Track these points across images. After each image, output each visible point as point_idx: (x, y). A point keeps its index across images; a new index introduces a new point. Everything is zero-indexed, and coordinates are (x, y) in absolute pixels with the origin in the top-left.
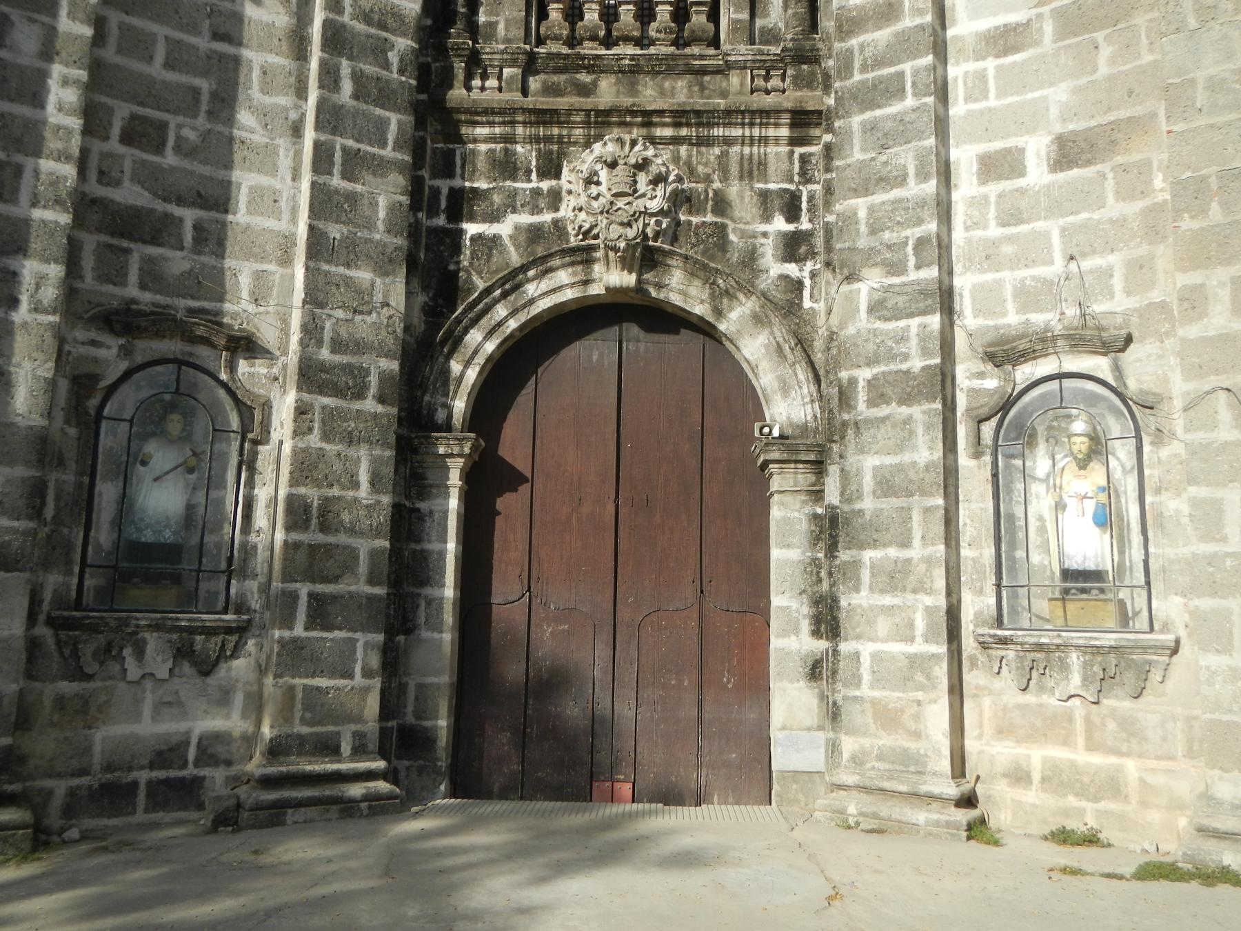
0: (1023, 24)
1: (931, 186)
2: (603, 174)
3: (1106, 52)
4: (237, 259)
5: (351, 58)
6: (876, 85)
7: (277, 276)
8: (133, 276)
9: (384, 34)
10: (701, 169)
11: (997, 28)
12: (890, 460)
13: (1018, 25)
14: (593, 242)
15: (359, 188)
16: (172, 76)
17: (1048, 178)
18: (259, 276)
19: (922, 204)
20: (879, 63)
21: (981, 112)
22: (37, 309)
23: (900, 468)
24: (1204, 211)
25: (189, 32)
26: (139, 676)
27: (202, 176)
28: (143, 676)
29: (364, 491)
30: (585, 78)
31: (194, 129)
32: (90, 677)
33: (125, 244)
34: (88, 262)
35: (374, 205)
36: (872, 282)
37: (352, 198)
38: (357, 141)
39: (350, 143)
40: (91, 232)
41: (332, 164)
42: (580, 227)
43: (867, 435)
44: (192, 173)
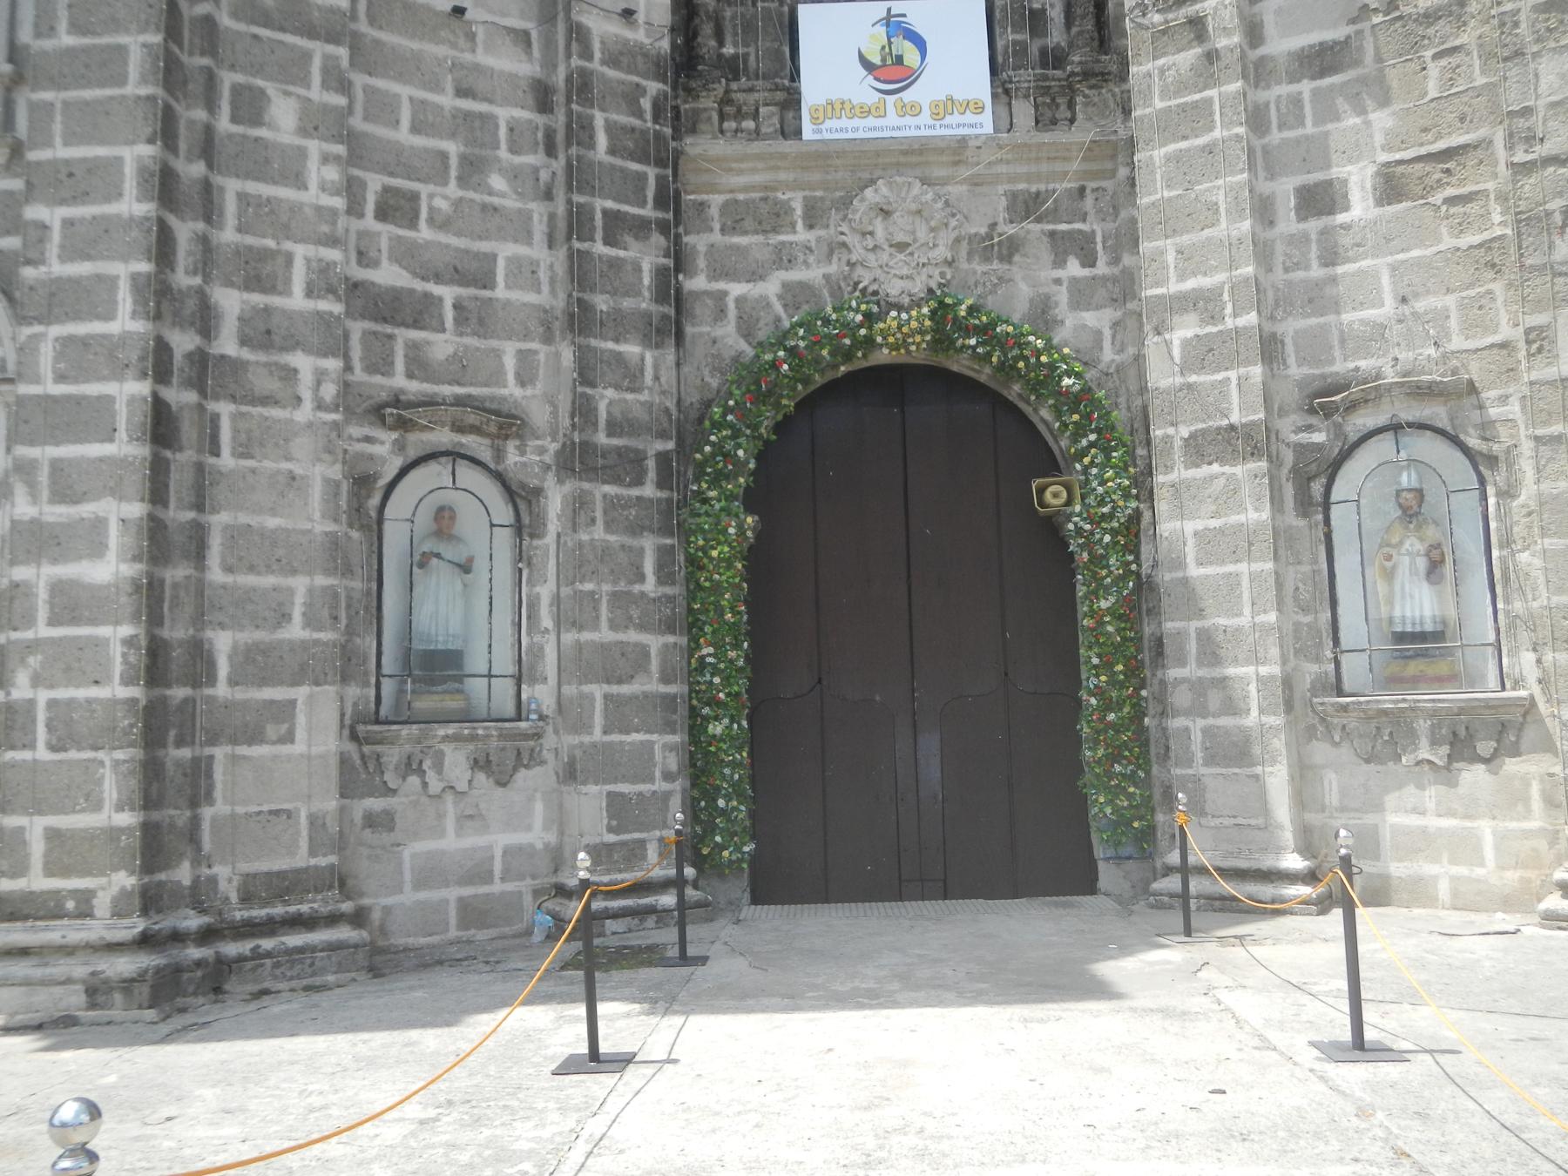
0: (1341, 42)
4: (499, 338)
5: (603, 110)
7: (542, 357)
8: (400, 365)
11: (1311, 46)
13: (1335, 43)
15: (622, 253)
16: (420, 141)
18: (522, 356)
21: (1298, 141)
22: (320, 406)
25: (432, 90)
26: (439, 790)
27: (457, 250)
28: (444, 790)
29: (650, 586)
31: (445, 197)
32: (394, 792)
33: (389, 329)
34: (356, 353)
35: (638, 269)
37: (615, 264)
38: (616, 199)
40: (355, 319)
41: (593, 228)
42: (856, 284)
44: (447, 246)
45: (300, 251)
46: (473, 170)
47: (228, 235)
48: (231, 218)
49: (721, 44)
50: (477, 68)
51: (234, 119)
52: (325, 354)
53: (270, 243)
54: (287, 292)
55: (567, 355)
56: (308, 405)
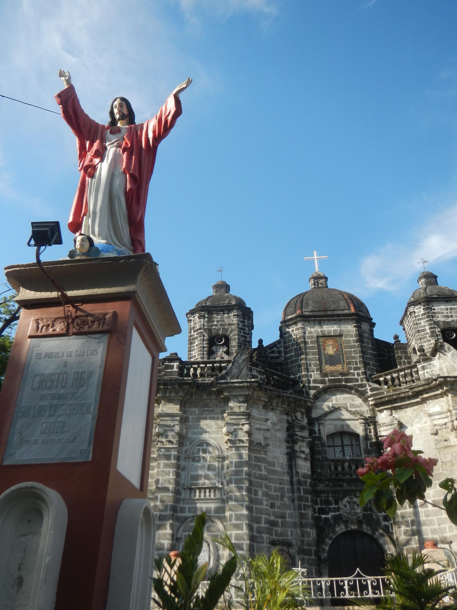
9: (306, 480)
14: (348, 519)
15: (306, 512)
18: (292, 532)
19: (410, 513)
30: (341, 483)
33: (272, 528)
35: (309, 515)
36: (403, 528)
37: (305, 514)
39: (304, 503)
45: (263, 516)
46: (282, 497)
48: (254, 512)
49: (318, 470)
50: (282, 479)
51: (254, 495)
53: (259, 515)
54: (261, 524)
55: (299, 531)
56: (265, 543)
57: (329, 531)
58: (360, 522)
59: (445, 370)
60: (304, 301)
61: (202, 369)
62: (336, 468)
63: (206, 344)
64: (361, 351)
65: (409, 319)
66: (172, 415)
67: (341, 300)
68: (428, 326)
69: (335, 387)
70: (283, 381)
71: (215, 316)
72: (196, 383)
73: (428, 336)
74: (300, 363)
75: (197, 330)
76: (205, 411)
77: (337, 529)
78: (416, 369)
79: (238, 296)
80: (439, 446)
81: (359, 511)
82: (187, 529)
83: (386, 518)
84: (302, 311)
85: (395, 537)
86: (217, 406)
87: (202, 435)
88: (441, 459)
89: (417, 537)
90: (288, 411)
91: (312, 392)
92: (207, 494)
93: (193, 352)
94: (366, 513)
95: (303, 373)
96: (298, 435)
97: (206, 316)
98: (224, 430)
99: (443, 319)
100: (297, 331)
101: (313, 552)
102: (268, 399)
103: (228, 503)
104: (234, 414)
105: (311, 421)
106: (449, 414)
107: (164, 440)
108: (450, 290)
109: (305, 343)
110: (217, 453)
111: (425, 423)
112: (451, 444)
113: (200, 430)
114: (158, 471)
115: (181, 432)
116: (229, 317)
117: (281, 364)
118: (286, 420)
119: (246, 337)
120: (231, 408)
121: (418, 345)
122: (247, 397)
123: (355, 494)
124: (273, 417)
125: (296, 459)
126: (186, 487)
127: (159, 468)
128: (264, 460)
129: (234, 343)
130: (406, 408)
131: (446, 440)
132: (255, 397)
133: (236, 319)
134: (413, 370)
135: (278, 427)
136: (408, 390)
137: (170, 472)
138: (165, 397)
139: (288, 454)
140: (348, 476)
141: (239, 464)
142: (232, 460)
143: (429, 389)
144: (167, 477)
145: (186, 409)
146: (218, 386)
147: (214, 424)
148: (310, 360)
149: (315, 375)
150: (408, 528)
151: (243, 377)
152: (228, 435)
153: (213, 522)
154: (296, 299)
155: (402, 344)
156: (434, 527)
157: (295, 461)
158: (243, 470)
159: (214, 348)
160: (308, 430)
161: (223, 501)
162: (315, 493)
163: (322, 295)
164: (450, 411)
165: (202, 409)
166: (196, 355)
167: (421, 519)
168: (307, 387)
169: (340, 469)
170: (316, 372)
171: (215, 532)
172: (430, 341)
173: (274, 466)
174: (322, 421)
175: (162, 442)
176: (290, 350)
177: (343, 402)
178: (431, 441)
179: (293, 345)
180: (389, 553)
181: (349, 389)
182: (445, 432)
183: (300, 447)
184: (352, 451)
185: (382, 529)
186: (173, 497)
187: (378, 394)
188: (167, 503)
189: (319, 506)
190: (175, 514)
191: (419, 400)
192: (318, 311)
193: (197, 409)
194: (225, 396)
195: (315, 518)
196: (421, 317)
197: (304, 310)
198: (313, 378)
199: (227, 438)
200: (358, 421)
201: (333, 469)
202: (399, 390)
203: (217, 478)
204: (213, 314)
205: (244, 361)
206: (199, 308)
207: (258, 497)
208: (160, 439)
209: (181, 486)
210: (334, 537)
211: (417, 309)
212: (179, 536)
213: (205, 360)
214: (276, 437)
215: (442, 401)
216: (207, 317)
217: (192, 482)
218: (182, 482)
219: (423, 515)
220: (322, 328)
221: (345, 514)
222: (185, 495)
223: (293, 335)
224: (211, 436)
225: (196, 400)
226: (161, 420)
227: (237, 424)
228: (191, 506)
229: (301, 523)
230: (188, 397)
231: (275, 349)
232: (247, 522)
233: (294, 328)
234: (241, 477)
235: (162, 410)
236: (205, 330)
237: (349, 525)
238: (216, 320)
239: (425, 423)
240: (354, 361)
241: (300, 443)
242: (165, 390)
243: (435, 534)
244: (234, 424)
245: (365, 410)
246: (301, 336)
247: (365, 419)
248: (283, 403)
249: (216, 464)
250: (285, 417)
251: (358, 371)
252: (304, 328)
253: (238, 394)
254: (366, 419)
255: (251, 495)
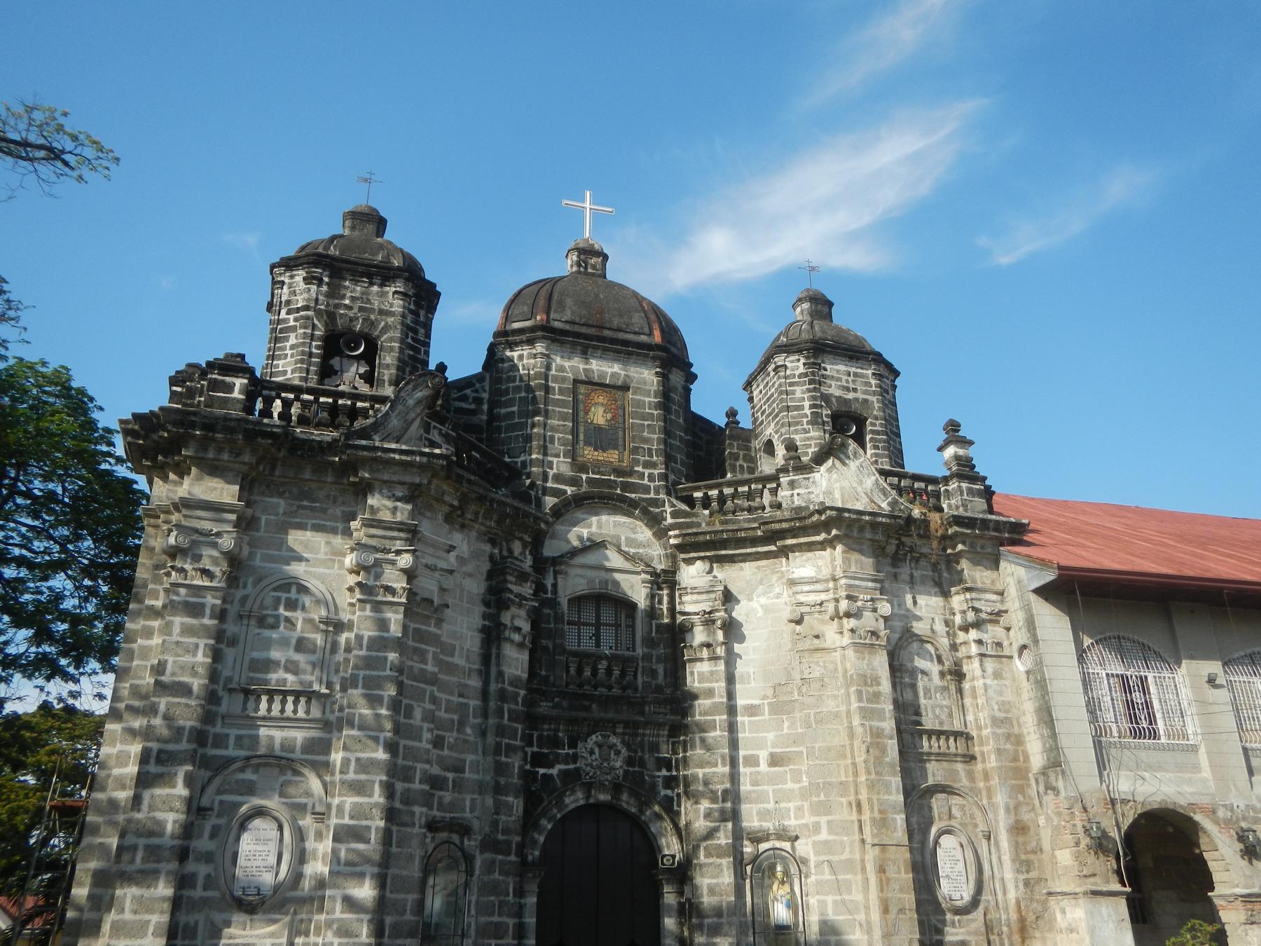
1: (727, 769)
2: (597, 750)
3: (786, 724)
6: (706, 721)
8: (435, 807)
10: (633, 747)
12: (714, 881)
17: (768, 769)
18: (473, 800)
19: (724, 775)
20: (706, 714)
22: (420, 827)
23: (717, 885)
24: (819, 795)
30: (587, 704)
33: (434, 792)
35: (514, 766)
36: (705, 805)
37: (507, 764)
39: (507, 741)
43: (704, 870)
46: (462, 724)
47: (400, 761)
48: (401, 756)
50: (466, 686)
52: (423, 806)
53: (411, 764)
54: (414, 782)
55: (489, 801)
56: (417, 826)
57: (550, 802)
58: (617, 788)
59: (837, 495)
60: (555, 297)
61: (305, 405)
62: (580, 671)
63: (318, 347)
64: (662, 429)
65: (768, 379)
66: (216, 508)
67: (636, 311)
68: (809, 400)
69: (600, 498)
70: (490, 465)
71: (347, 283)
72: (290, 438)
73: (805, 420)
74: (529, 431)
75: (298, 310)
76: (304, 508)
77: (567, 800)
78: (774, 485)
79: (406, 249)
80: (800, 646)
81: (618, 764)
82: (227, 787)
83: (671, 782)
84: (548, 317)
85: (683, 822)
86: (335, 502)
87: (289, 565)
88: (802, 672)
89: (730, 825)
90: (496, 534)
91: (550, 501)
92: (290, 707)
93: (281, 362)
94: (631, 769)
95: (534, 456)
96: (511, 592)
97: (326, 279)
98: (350, 560)
99: (838, 393)
100: (532, 361)
101: (514, 846)
102: (460, 501)
103: (340, 730)
104: (379, 524)
105: (541, 564)
106: (831, 585)
107: (187, 567)
108: (856, 336)
109: (547, 389)
110: (323, 613)
111: (778, 596)
112: (826, 646)
113: (284, 553)
114: (164, 641)
115: (237, 550)
116: (383, 295)
117: (476, 429)
118: (487, 554)
119: (417, 351)
120: (373, 510)
121: (781, 435)
122: (416, 489)
123: (614, 727)
124: (462, 542)
125: (503, 643)
126: (237, 686)
127: (170, 634)
128: (434, 640)
129: (388, 360)
130: (744, 561)
131: (817, 637)
132: (432, 492)
133: (401, 302)
134: (768, 486)
135: (469, 568)
136: (756, 525)
137: (197, 646)
138: (202, 459)
139: (484, 630)
140: (604, 690)
141: (380, 643)
142: (361, 633)
143: (799, 528)
144: (187, 659)
145: (255, 497)
146: (348, 452)
147: (323, 543)
148: (553, 429)
149: (560, 465)
150: (715, 806)
151: (411, 439)
152: (358, 573)
153: (296, 773)
154: (535, 288)
155: (742, 428)
156: (765, 806)
157: (499, 647)
158: (386, 658)
159: (335, 362)
160: (532, 581)
161: (329, 726)
162: (531, 719)
163: (596, 290)
164: (835, 580)
165: (297, 503)
166: (289, 369)
167: (742, 788)
168: (540, 487)
169: (587, 673)
170: (562, 459)
171: (301, 796)
172: (809, 432)
173: (453, 656)
174: (563, 567)
175: (182, 570)
176: (510, 399)
177: (612, 532)
178: (785, 636)
179: (518, 389)
180: (667, 853)
181: (629, 506)
182: (818, 619)
183: (513, 617)
184: (616, 636)
185: (660, 804)
186: (199, 710)
187: (689, 525)
188: (181, 723)
189: (535, 749)
190: (201, 751)
191: (773, 548)
192: (583, 325)
193: (282, 502)
194: (363, 479)
195: (525, 774)
196: (797, 379)
197: (552, 316)
198: (555, 471)
199: (352, 580)
200: (639, 577)
201: (572, 671)
202: (734, 522)
203: (317, 672)
204: (345, 279)
205: (419, 402)
206: (307, 255)
207: (412, 721)
208: (178, 564)
209: (221, 683)
210: (559, 816)
211: (792, 362)
212: (205, 802)
213: (312, 384)
214: (462, 590)
215: (821, 558)
216: (328, 284)
217: (251, 675)
218: (226, 673)
219: (748, 781)
220: (587, 364)
221: (589, 768)
222: (229, 704)
223: (521, 368)
224: (313, 569)
225: (282, 480)
226: (185, 516)
227: (385, 549)
228: (243, 732)
229: (497, 783)
230: (264, 469)
231: (468, 391)
232: (384, 778)
233: (525, 353)
234: (382, 673)
235: (189, 493)
236: (319, 313)
237: (593, 792)
238: (349, 294)
239: (778, 596)
240: (646, 446)
241: (513, 610)
242: (204, 444)
243: (766, 821)
244: (376, 549)
245: (656, 553)
246: (540, 372)
247: (654, 574)
248: (487, 516)
249: (319, 639)
250: (487, 548)
251: (651, 471)
252: (548, 356)
253: (395, 478)
254: (656, 573)
255: (397, 718)
